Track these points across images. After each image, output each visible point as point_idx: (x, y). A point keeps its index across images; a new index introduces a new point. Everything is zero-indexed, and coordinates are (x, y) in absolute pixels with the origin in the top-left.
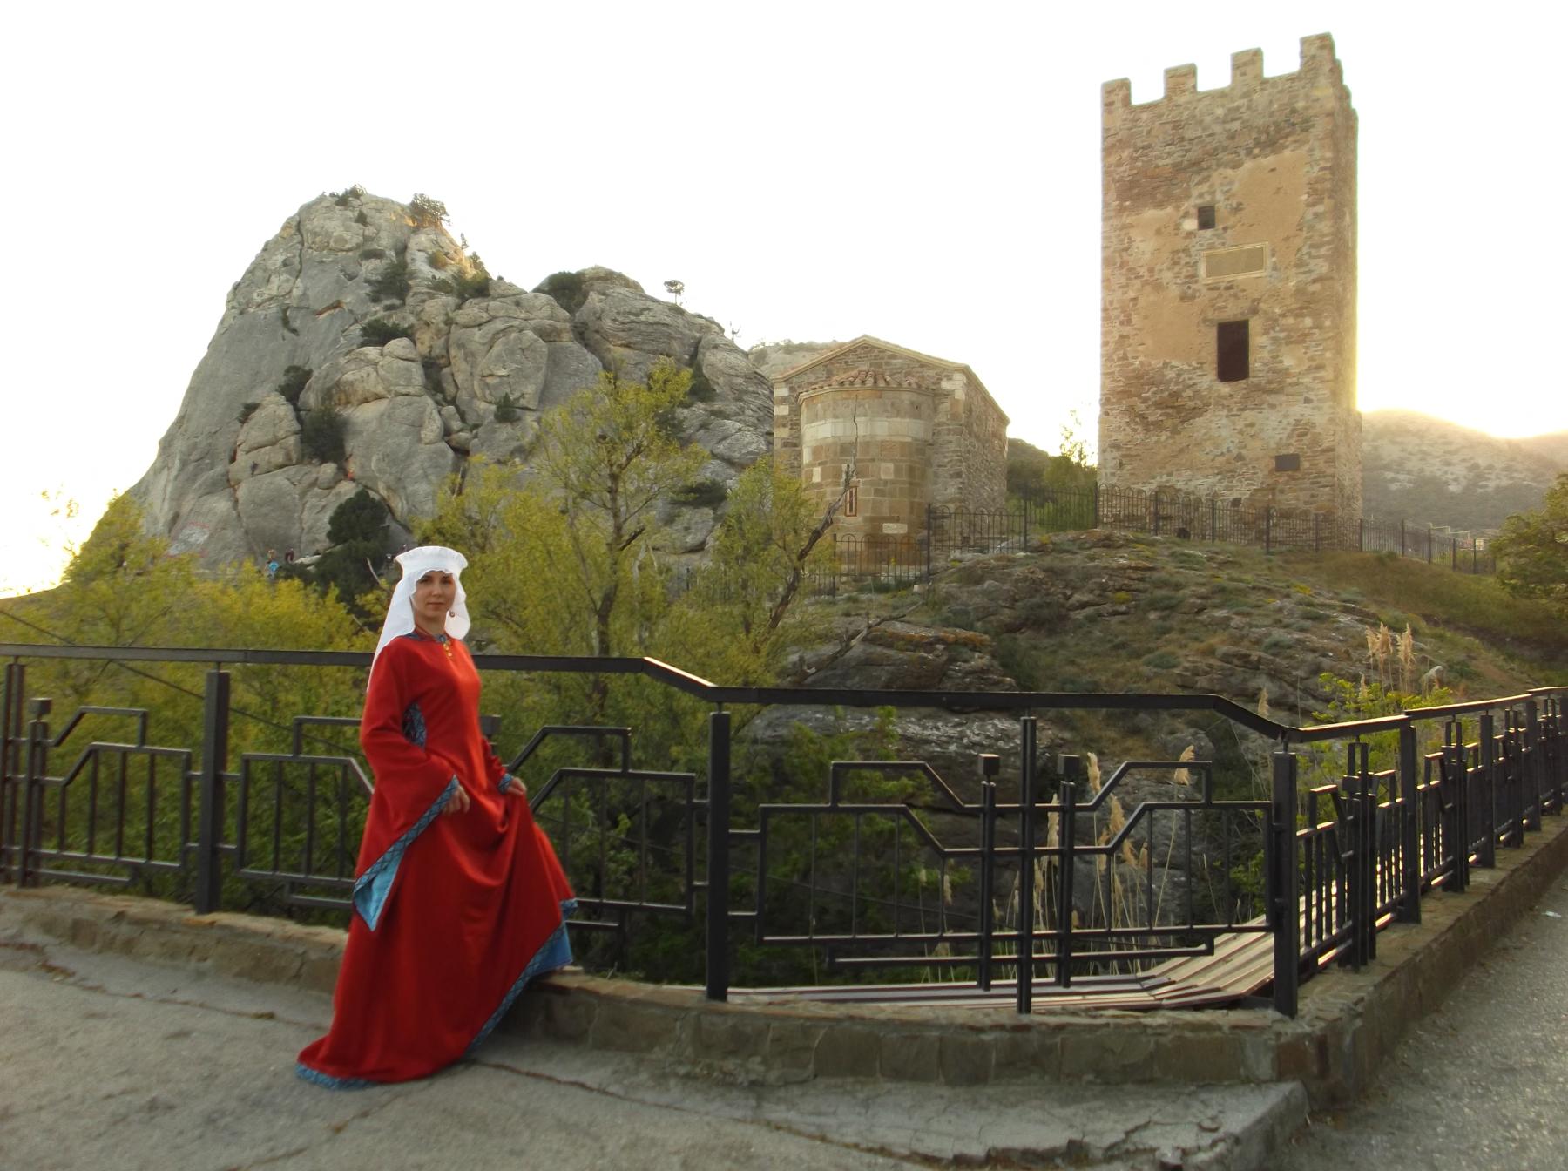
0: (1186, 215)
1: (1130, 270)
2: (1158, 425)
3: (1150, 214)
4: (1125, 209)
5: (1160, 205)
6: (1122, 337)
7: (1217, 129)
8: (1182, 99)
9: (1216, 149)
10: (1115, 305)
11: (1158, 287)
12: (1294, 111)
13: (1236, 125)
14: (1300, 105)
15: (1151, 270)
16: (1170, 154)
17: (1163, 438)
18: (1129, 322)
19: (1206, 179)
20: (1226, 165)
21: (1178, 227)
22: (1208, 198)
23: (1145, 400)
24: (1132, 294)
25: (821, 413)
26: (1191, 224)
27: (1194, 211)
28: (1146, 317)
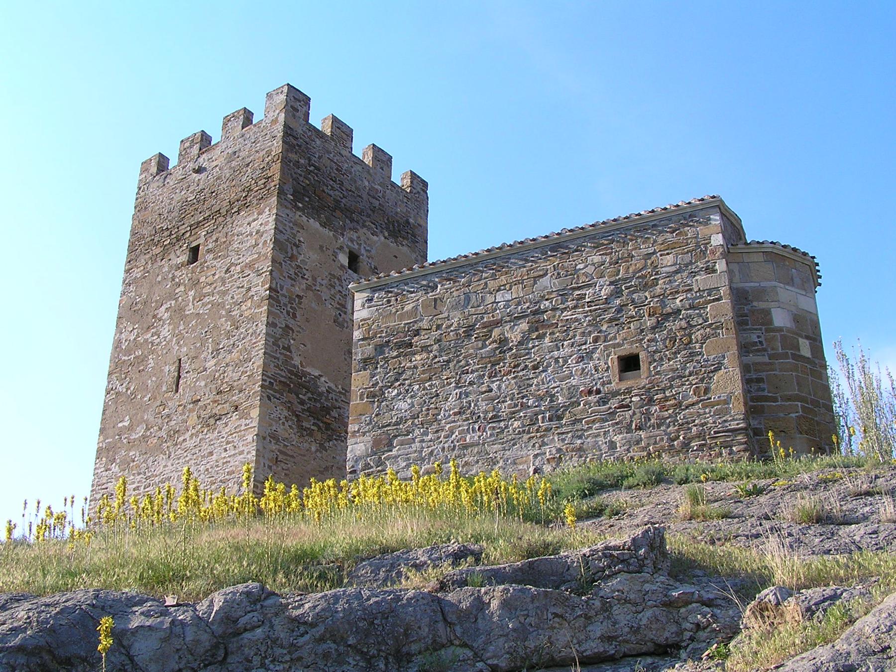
0: (341, 248)
1: (298, 267)
2: (311, 433)
3: (314, 224)
4: (298, 208)
5: (323, 225)
6: (287, 326)
7: (365, 196)
8: (344, 152)
9: (362, 211)
10: (284, 292)
11: (319, 299)
12: (408, 222)
13: (376, 203)
14: (411, 220)
15: (314, 279)
16: (333, 188)
17: (313, 449)
18: (294, 316)
19: (355, 230)
20: (368, 229)
21: (335, 255)
22: (356, 247)
23: (302, 403)
24: (297, 290)
25: (797, 280)
26: (344, 259)
27: (348, 251)
28: (307, 320)
